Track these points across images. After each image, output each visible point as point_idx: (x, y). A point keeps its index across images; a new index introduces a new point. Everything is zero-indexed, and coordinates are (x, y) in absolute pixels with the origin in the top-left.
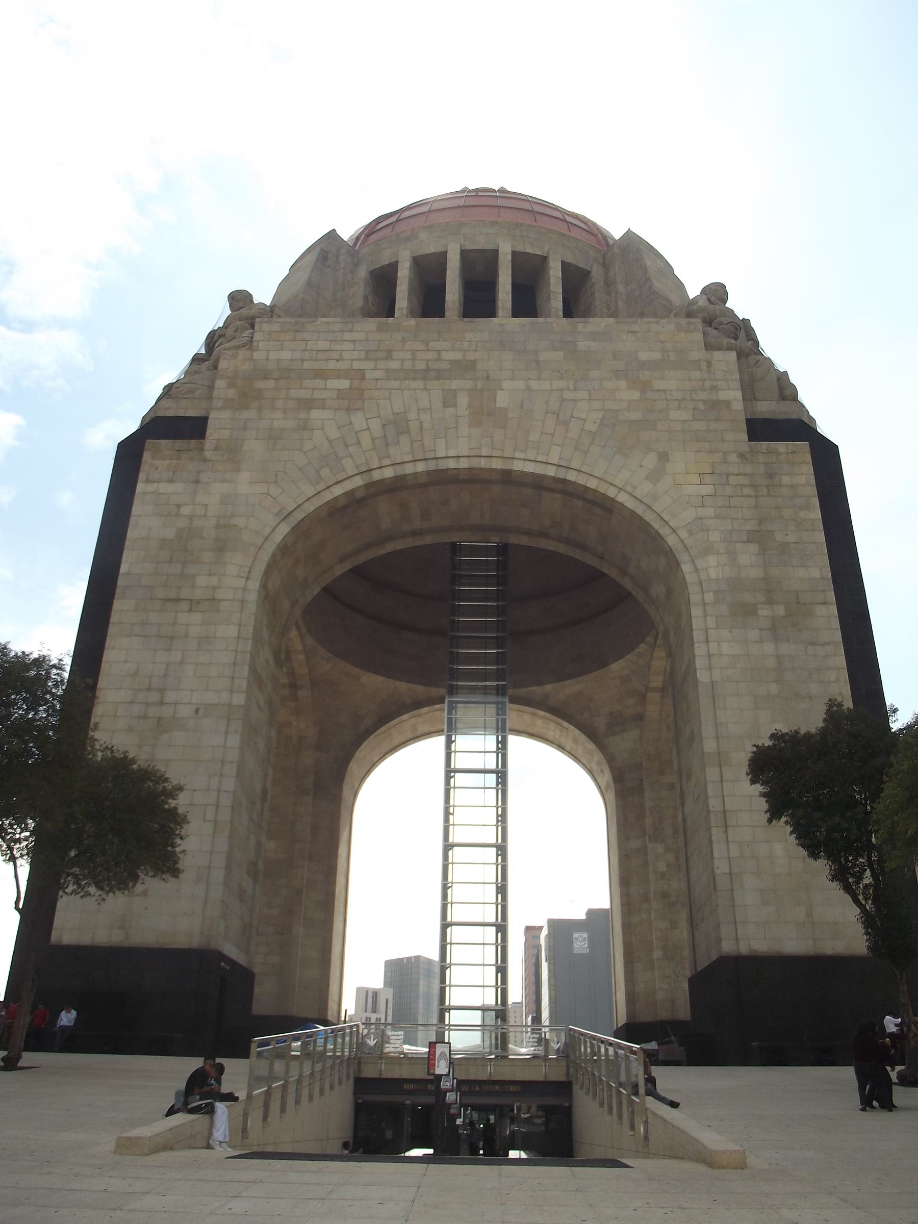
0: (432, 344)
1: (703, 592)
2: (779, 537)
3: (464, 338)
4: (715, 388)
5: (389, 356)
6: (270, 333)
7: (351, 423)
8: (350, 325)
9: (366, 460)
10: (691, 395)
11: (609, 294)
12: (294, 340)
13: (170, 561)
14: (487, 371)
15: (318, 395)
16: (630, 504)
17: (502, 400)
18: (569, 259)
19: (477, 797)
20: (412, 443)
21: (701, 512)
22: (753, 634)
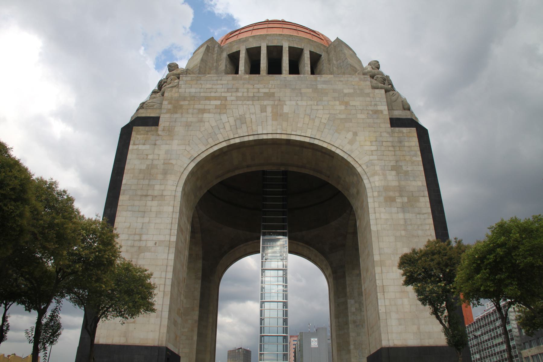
0: (255, 86)
1: (373, 192)
2: (404, 168)
3: (269, 83)
4: (376, 105)
5: (237, 90)
6: (186, 81)
8: (220, 78)
9: (228, 135)
10: (366, 107)
11: (330, 64)
12: (197, 84)
13: (144, 179)
14: (279, 97)
15: (207, 107)
17: (286, 109)
18: (313, 50)
20: (247, 127)
21: (372, 157)
22: (394, 210)
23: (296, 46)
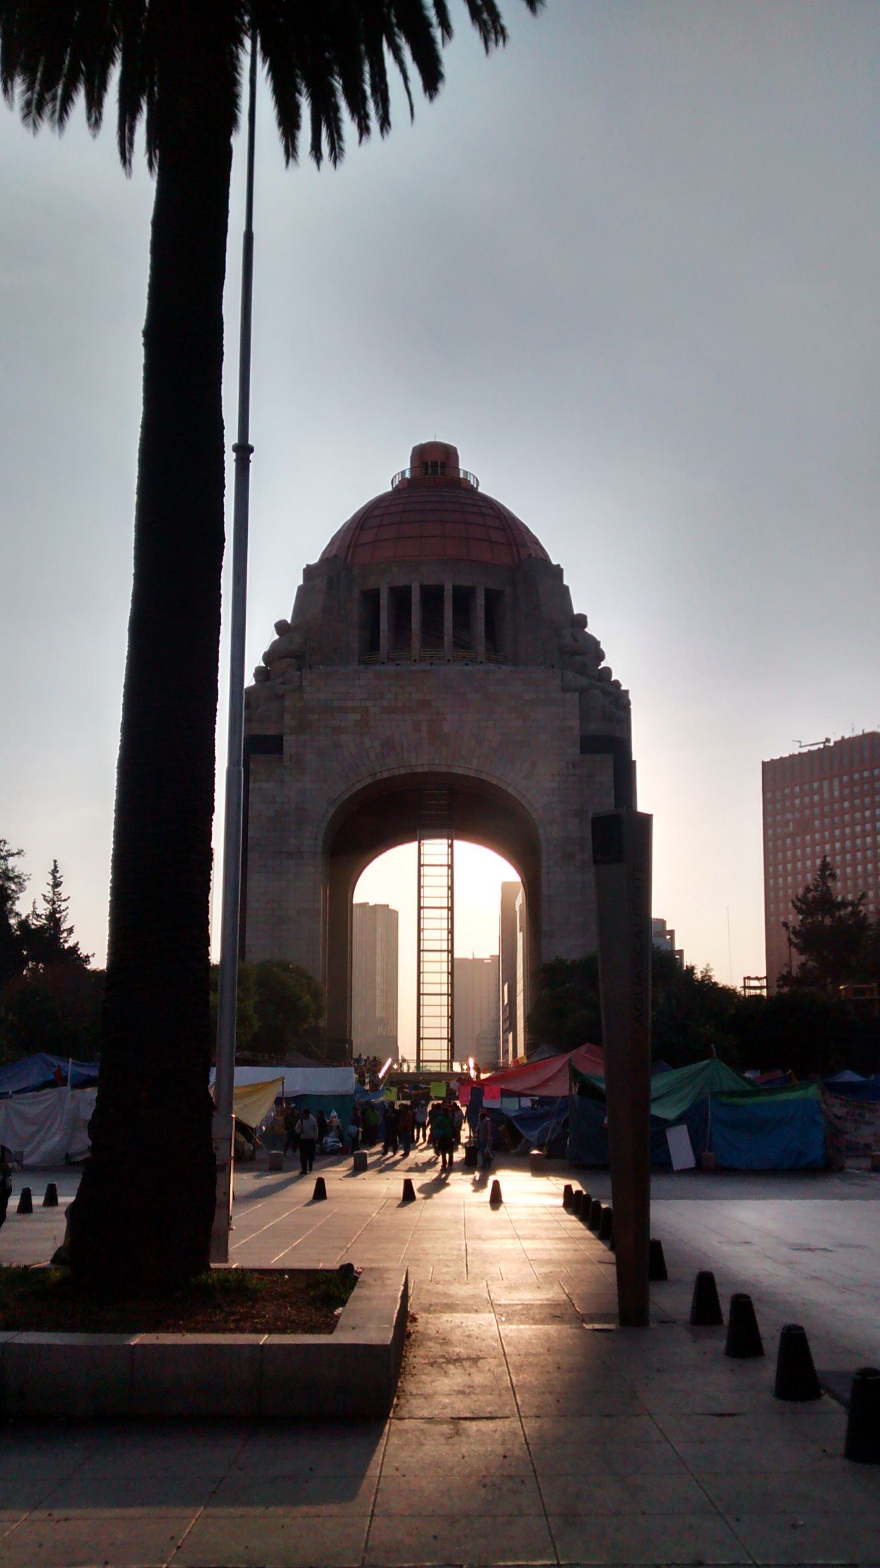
16: (514, 793)
19: (436, 924)
23: (464, 584)
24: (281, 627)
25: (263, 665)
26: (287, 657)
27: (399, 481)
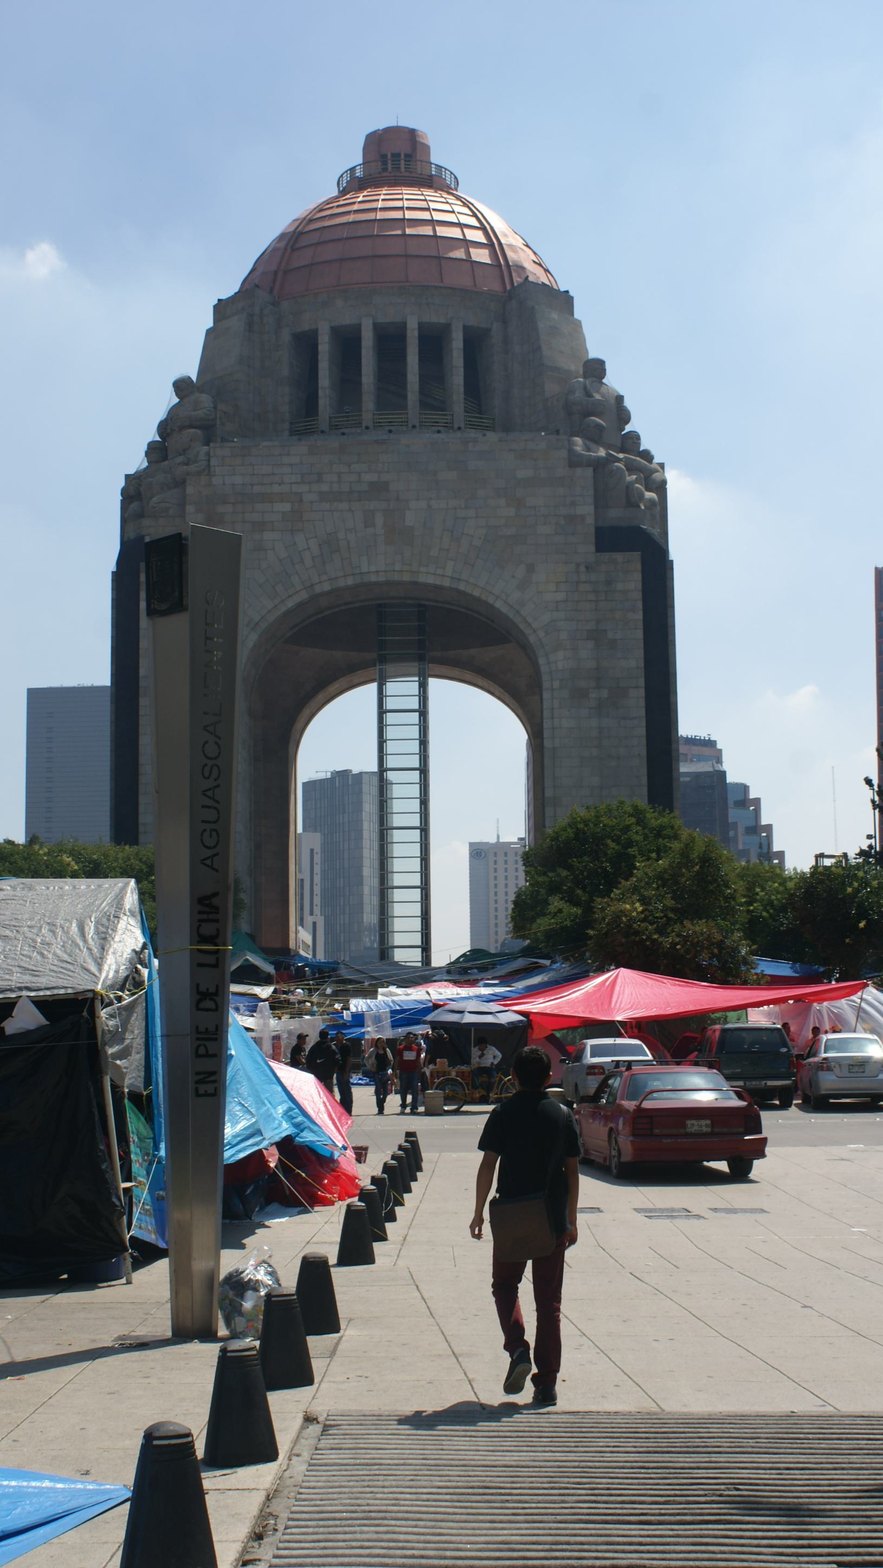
2: (610, 635)
5: (320, 480)
7: (295, 544)
16: (504, 609)
18: (472, 322)
23: (434, 319)
24: (181, 386)
25: (158, 439)
26: (191, 427)
27: (347, 182)
